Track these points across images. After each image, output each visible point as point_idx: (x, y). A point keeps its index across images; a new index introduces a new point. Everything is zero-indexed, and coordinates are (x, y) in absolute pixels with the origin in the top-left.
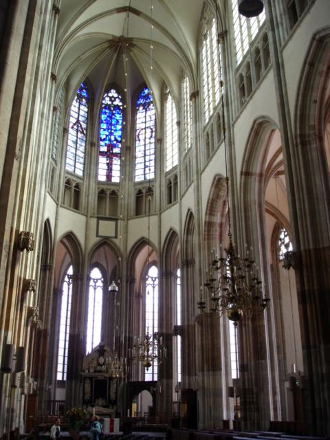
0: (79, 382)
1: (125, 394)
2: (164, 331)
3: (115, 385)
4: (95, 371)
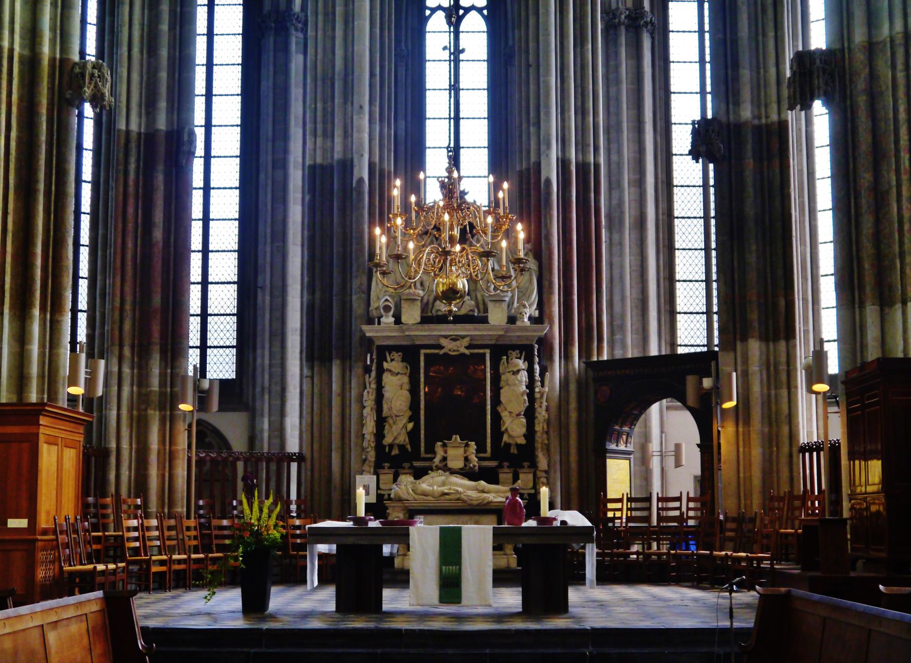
0: (358, 370)
1: (574, 415)
2: (746, 113)
3: (524, 376)
4: (426, 320)
